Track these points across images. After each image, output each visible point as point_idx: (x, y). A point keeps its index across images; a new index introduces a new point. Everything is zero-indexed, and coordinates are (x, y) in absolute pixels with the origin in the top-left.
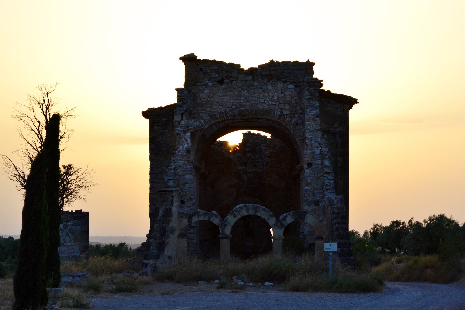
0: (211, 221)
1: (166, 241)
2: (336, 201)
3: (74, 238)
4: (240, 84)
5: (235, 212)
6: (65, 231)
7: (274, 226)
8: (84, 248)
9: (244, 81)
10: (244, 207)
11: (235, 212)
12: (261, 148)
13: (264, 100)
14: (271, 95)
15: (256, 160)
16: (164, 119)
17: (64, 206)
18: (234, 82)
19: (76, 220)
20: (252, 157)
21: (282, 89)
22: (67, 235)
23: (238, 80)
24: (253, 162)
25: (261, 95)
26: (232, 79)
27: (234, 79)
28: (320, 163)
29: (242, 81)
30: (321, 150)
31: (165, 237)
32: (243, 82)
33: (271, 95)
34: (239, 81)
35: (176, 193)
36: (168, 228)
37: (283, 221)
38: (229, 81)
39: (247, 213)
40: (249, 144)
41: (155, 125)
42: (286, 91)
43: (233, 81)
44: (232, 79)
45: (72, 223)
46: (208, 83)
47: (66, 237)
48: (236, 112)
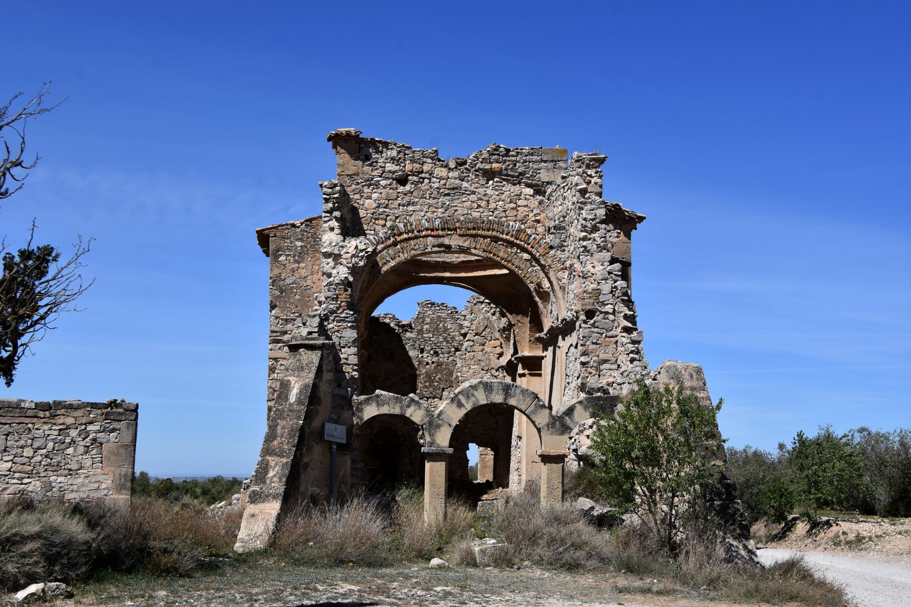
0: (407, 415)
1: (306, 460)
2: (687, 373)
3: (101, 457)
4: (436, 185)
5: (461, 397)
6: (82, 443)
7: (546, 428)
8: (123, 480)
9: (444, 179)
10: (481, 386)
11: (461, 397)
12: (446, 325)
13: (479, 214)
14: (492, 206)
15: (439, 344)
16: (299, 244)
17: (19, 358)
18: (426, 181)
19: (107, 421)
20: (432, 339)
21: (512, 195)
22: (86, 452)
23: (433, 177)
24: (434, 347)
25: (475, 205)
26: (423, 175)
27: (427, 175)
28: (611, 311)
29: (441, 179)
30: (613, 285)
31: (303, 449)
32: (443, 182)
33: (492, 206)
34: (434, 180)
35: (328, 352)
36: (309, 428)
37: (567, 418)
38: (415, 178)
39: (487, 399)
40: (428, 320)
41: (281, 255)
42: (519, 200)
43: (426, 178)
44: (423, 175)
45: (98, 428)
46: (379, 181)
47: (84, 457)
48: (437, 223)
